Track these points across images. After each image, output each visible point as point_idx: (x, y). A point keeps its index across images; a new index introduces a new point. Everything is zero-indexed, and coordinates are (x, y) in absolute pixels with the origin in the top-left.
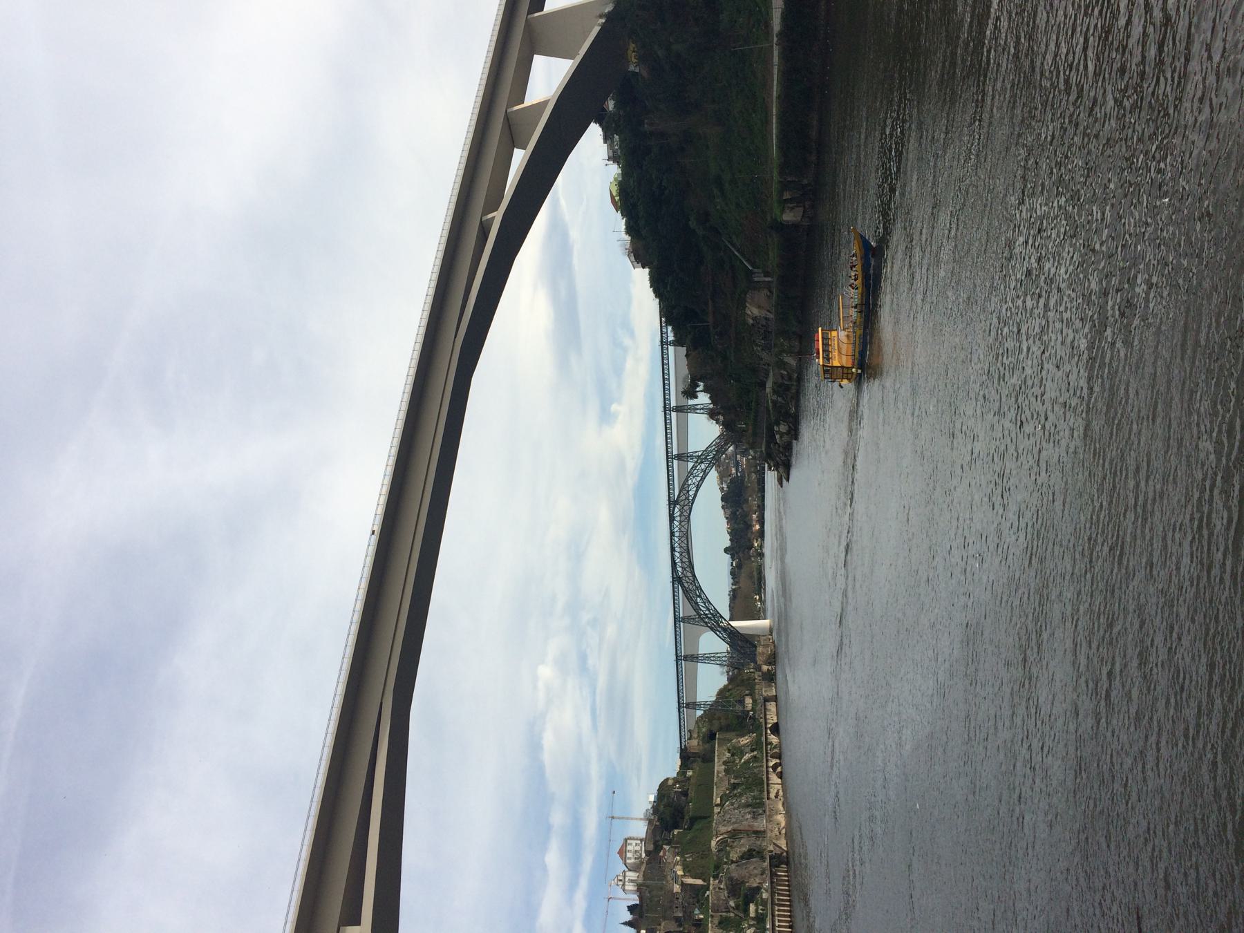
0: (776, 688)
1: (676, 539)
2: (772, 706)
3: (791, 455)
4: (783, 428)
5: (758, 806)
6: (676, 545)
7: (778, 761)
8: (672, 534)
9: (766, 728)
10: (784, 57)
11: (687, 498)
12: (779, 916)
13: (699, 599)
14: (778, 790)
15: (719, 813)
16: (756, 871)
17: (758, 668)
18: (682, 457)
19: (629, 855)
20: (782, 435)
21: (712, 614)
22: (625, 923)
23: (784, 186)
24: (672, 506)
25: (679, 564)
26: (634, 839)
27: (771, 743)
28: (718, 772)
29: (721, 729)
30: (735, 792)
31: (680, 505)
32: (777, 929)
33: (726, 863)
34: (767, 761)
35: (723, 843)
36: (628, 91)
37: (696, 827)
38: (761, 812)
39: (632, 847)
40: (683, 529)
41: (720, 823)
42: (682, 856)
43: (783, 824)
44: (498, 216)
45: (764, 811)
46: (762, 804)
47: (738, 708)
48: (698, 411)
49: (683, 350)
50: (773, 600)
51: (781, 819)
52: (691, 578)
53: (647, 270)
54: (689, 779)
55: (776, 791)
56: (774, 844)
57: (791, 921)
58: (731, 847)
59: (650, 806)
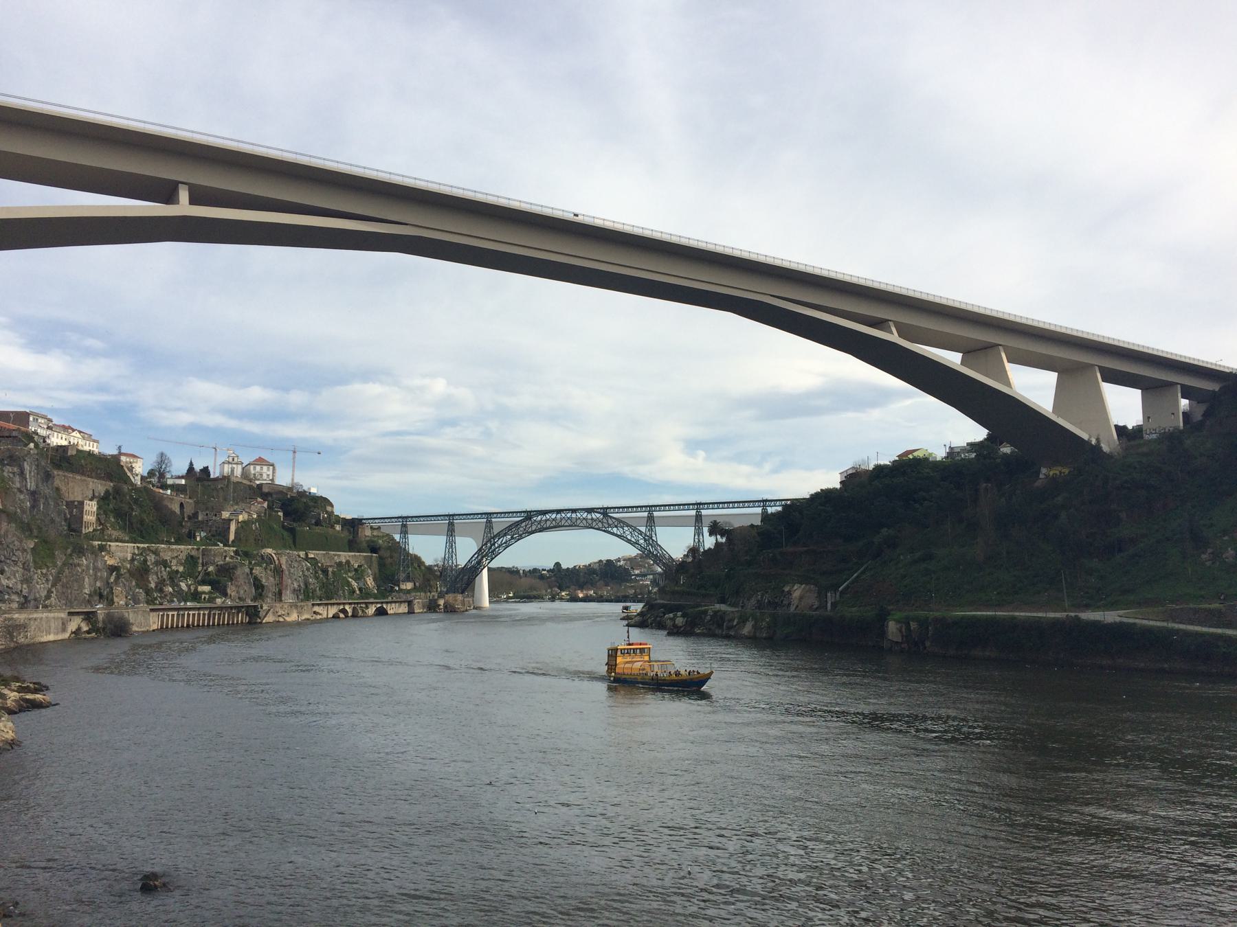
0: (422, 612)
1: (569, 515)
2: (404, 608)
3: (652, 628)
4: (680, 621)
5: (306, 594)
6: (563, 515)
7: (350, 614)
8: (574, 511)
9: (382, 603)
10: (1055, 623)
11: (609, 526)
12: (199, 614)
13: (509, 537)
14: (320, 614)
15: (299, 556)
16: (242, 592)
17: (441, 595)
18: (651, 520)
19: (258, 468)
20: (673, 619)
21: (495, 550)
22: (191, 464)
23: (924, 623)
24: (602, 511)
25: (544, 518)
26: (274, 472)
27: (367, 608)
28: (339, 556)
29: (381, 558)
30: (320, 572)
31: (604, 519)
32: (186, 613)
33: (250, 563)
34: (350, 604)
35: (270, 560)
36: (1019, 467)
37: (285, 533)
38: (300, 597)
39: (265, 470)
40: (579, 521)
41: (289, 557)
42: (256, 520)
43: (288, 619)
44: (894, 337)
45: (302, 601)
46: (307, 598)
47: (402, 576)
48: (696, 537)
49: (758, 522)
50: (510, 610)
51: (293, 617)
52: (530, 530)
53: (838, 486)
54: (333, 527)
55: (321, 612)
56: (269, 610)
57: (193, 626)
58: (266, 569)
59: (305, 488)
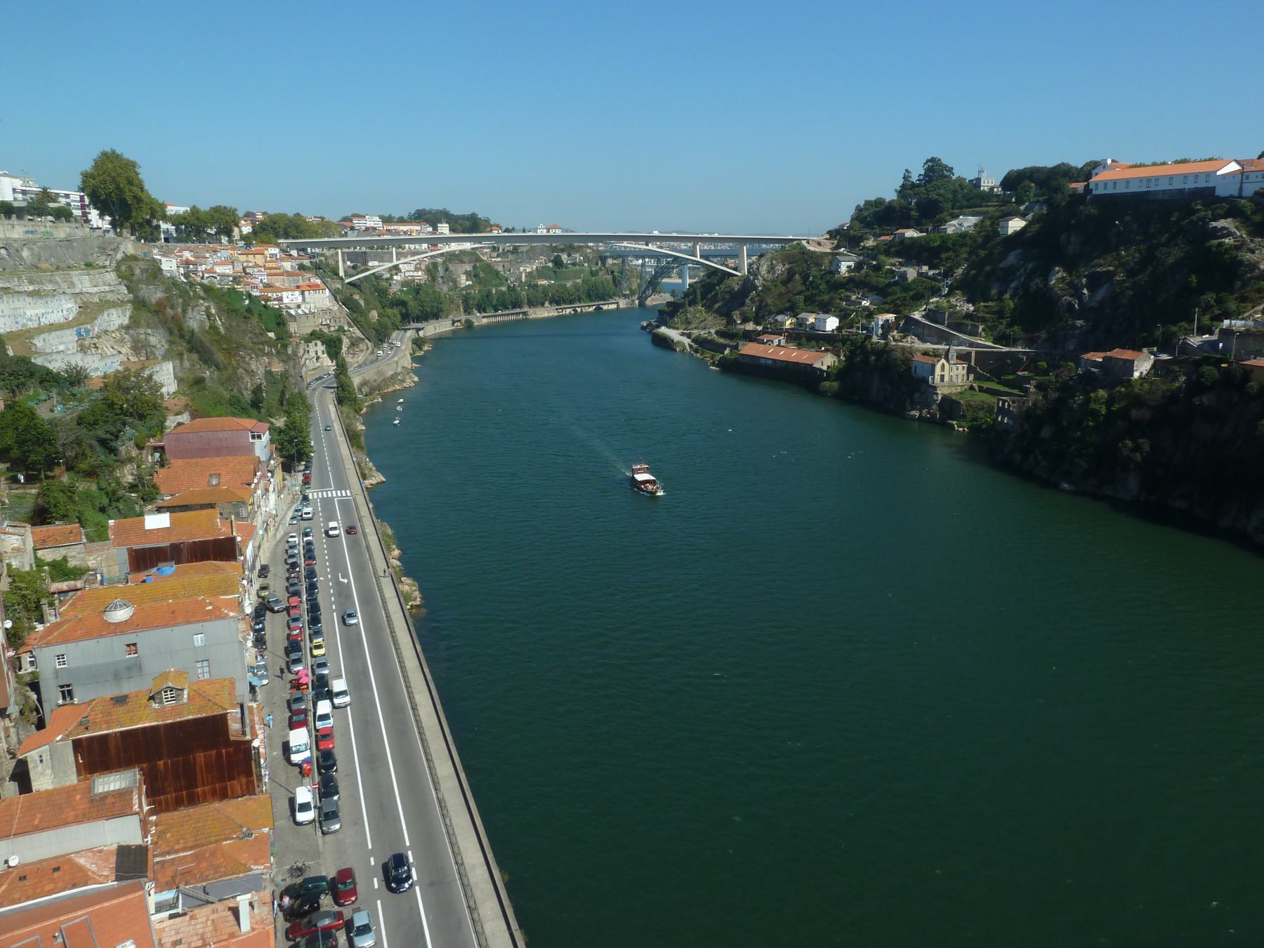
19: (554, 230)
